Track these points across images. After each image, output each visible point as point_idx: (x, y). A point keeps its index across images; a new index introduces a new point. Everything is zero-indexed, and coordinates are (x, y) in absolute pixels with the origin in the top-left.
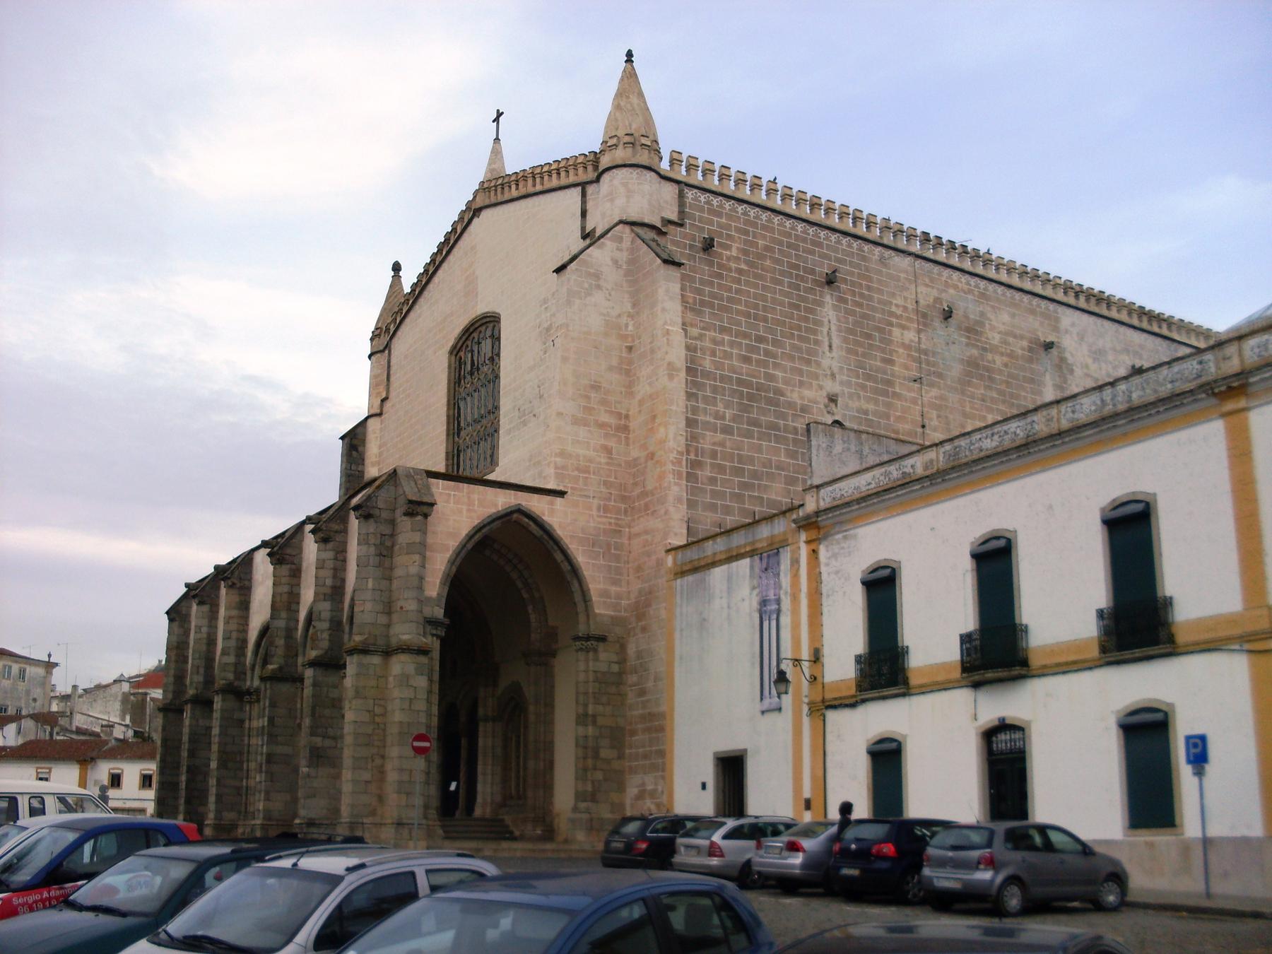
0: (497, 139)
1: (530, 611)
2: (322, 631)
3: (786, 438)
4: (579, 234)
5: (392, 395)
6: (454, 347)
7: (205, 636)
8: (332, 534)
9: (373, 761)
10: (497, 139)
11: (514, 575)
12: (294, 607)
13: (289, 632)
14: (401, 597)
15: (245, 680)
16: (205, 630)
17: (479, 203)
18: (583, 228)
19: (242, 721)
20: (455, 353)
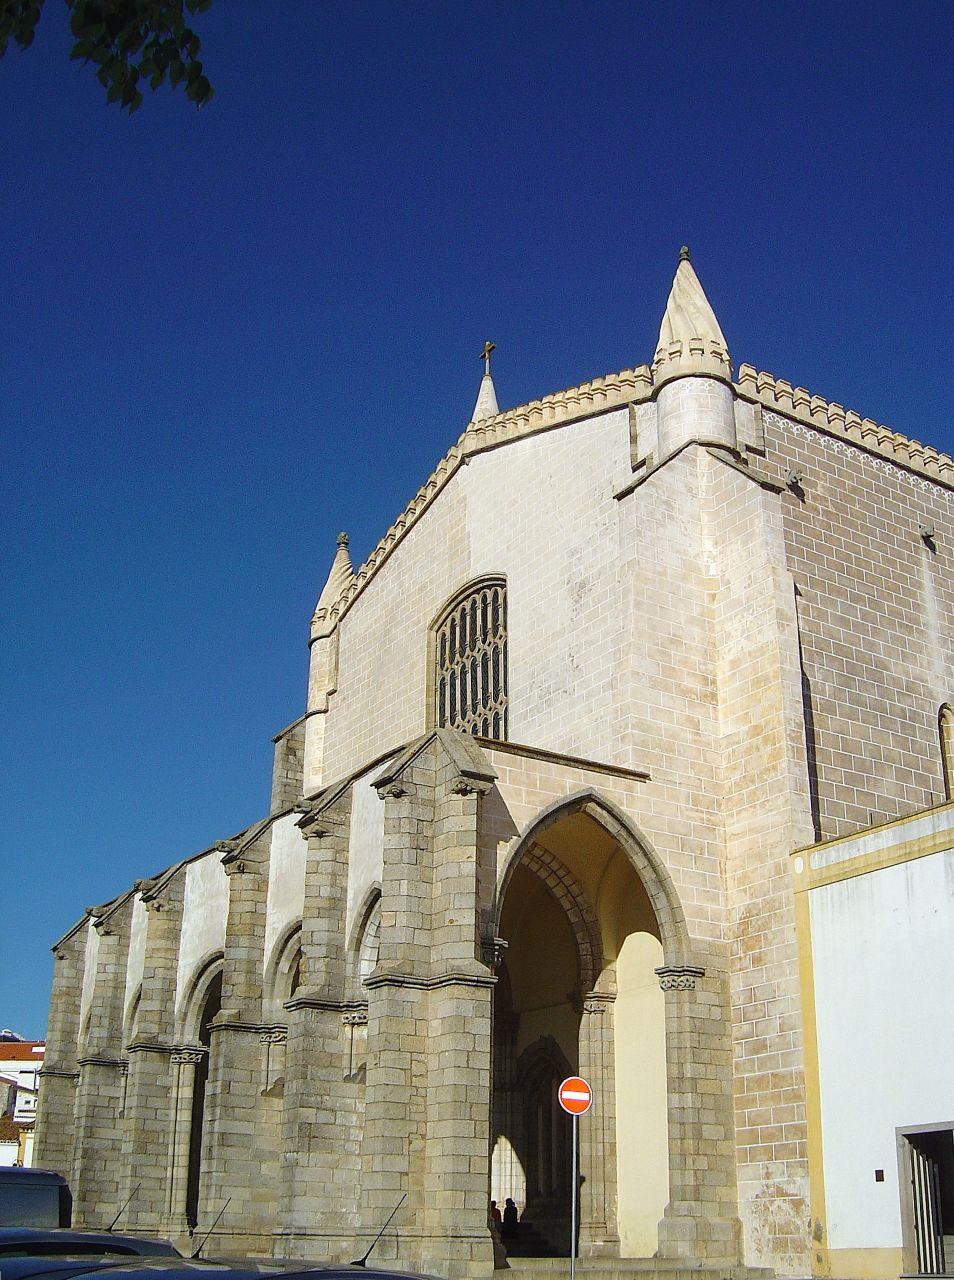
3: (894, 722)
7: (111, 976)
9: (410, 1143)
11: (558, 892)
12: (258, 931)
13: (252, 966)
15: (173, 1033)
16: (111, 969)
18: (633, 456)
19: (168, 1089)
20: (436, 627)
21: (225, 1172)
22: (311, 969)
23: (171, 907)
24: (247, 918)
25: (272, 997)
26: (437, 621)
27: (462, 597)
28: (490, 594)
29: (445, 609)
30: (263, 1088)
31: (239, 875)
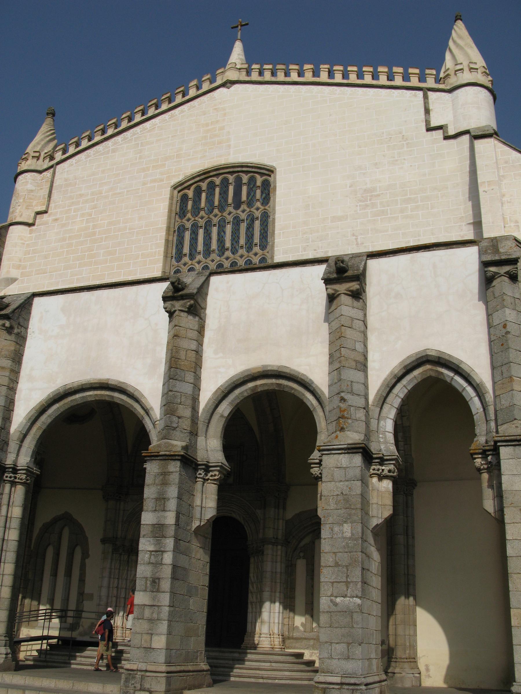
4: (423, 127)
6: (181, 184)
13: (195, 399)
18: (428, 122)
20: (180, 188)
22: (353, 417)
23: (19, 331)
27: (215, 173)
29: (193, 178)
31: (186, 314)
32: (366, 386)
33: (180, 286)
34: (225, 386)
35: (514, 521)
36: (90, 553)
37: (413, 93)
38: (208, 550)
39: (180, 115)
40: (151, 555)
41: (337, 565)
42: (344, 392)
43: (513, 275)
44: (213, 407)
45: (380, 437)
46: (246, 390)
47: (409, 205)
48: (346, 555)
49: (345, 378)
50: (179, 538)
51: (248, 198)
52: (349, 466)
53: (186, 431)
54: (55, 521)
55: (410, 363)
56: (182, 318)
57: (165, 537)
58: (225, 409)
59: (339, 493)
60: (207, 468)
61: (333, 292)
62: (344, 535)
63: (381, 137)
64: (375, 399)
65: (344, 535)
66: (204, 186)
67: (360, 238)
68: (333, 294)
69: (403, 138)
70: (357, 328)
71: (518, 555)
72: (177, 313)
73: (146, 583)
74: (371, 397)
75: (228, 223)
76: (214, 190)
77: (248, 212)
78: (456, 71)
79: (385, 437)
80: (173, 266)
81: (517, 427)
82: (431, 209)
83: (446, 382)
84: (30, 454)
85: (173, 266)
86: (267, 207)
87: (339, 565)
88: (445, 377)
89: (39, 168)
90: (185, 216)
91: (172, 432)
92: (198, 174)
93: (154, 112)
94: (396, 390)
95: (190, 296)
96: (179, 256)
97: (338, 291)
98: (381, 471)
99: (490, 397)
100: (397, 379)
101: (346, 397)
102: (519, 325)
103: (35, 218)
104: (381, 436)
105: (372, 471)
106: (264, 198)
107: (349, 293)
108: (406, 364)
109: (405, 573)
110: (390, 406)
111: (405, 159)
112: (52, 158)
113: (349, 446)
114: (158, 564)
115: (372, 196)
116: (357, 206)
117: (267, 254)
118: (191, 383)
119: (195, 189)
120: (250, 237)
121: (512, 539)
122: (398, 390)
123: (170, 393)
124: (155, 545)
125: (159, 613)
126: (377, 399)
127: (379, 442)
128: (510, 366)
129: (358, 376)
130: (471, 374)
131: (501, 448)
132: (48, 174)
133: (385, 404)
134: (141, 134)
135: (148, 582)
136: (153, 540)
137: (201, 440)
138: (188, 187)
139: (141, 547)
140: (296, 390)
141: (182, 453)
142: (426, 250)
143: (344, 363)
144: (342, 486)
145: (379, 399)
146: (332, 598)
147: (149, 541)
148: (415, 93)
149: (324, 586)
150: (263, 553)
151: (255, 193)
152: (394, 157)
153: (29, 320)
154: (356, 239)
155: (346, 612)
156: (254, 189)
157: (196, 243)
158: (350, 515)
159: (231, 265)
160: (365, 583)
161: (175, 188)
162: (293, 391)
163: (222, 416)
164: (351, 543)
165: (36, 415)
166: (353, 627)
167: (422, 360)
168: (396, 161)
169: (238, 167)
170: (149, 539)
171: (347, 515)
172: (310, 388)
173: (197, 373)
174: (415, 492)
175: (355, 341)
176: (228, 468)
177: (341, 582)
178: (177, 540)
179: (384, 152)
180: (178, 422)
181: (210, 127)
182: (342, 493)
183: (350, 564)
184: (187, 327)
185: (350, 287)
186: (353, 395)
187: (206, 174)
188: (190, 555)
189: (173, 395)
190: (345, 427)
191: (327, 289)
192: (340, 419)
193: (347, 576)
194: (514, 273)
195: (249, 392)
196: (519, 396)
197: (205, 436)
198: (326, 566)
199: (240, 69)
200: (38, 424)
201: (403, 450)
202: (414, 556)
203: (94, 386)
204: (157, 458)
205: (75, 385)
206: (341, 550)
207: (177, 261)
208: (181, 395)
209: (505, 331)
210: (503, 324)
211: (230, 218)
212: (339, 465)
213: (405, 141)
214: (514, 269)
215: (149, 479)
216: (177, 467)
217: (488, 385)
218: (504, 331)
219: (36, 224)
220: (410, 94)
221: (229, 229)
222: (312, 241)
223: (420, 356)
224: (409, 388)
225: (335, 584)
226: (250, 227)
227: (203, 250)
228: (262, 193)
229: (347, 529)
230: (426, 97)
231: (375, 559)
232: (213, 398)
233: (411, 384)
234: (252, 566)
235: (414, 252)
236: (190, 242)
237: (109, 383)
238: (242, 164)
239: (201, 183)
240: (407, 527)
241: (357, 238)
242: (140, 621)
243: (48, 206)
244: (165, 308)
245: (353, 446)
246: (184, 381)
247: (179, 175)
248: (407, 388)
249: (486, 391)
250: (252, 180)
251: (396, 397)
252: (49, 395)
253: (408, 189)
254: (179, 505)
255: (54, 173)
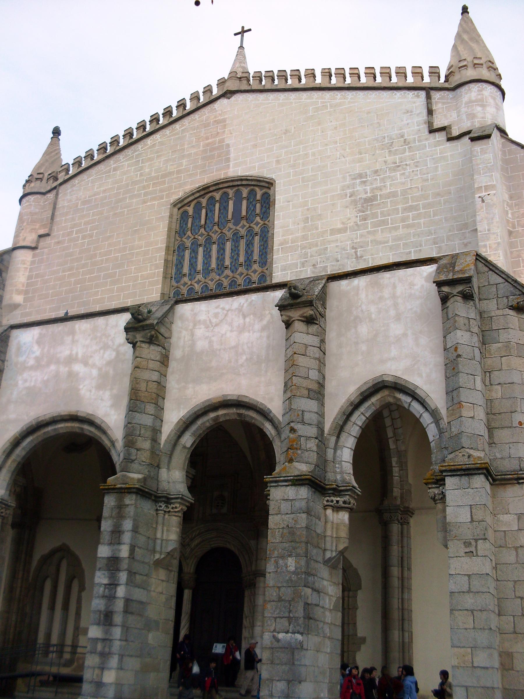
0: (241, 47)
1: (394, 464)
2: (308, 438)
5: (58, 232)
6: (181, 201)
8: (318, 315)
10: (241, 47)
13: (156, 431)
14: (519, 409)
17: (232, 86)
18: (430, 124)
20: (179, 205)
21: (126, 640)
22: (303, 447)
24: (153, 387)
25: (168, 469)
26: (183, 200)
28: (245, 192)
29: (193, 194)
30: (157, 556)
32: (321, 415)
33: (140, 317)
34: (187, 417)
35: (457, 555)
36: (86, 585)
37: (416, 94)
38: (173, 583)
39: (181, 129)
40: (105, 589)
41: (280, 600)
42: (294, 422)
43: (466, 294)
44: (175, 438)
45: (336, 467)
46: (208, 421)
47: (411, 214)
48: (289, 590)
49: (295, 408)
50: (134, 571)
51: (247, 212)
52: (295, 498)
53: (144, 463)
54: (53, 552)
55: (366, 390)
56: (144, 349)
57: (120, 571)
58: (188, 440)
59: (285, 526)
60: (168, 500)
61: (287, 318)
62: (288, 569)
63: (383, 142)
64: (331, 428)
65: (288, 569)
66: (204, 201)
67: (360, 250)
68: (288, 321)
69: (405, 142)
70: (311, 355)
71: (460, 590)
72: (138, 344)
73: (100, 616)
74: (327, 427)
75: (227, 239)
76: (214, 206)
77: (247, 228)
78: (459, 68)
79: (342, 467)
80: (173, 286)
81: (463, 455)
82: (433, 217)
83: (404, 408)
84: (5, 487)
85: (173, 286)
86: (266, 222)
87: (283, 600)
88: (403, 403)
89: (43, 191)
90: (185, 234)
91: (130, 464)
92: (198, 190)
93: (155, 127)
94: (354, 418)
95: (151, 327)
96: (179, 275)
97: (292, 318)
98: (335, 502)
99: (444, 423)
100: (353, 406)
101: (295, 427)
102: (472, 347)
103: (38, 242)
104: (337, 466)
105: (326, 503)
106: (264, 213)
107: (303, 319)
108: (362, 390)
109: (399, 607)
110: (347, 434)
111: (406, 165)
112: (56, 179)
113: (296, 478)
114: (111, 598)
115: (372, 205)
116: (357, 217)
117: (266, 271)
118: (151, 415)
119: (195, 205)
120: (249, 253)
121: (454, 573)
122: (356, 418)
123: (129, 425)
124: (110, 578)
125: (110, 647)
126: (333, 428)
127: (335, 472)
128: (459, 392)
129: (312, 405)
130: (426, 400)
131: (446, 478)
132: (52, 195)
133: (342, 432)
134: (142, 151)
135: (102, 616)
136: (108, 573)
137: (163, 473)
138: (188, 204)
139: (97, 580)
140: (256, 419)
141: (137, 486)
142: (386, 270)
143: (295, 392)
144: (287, 519)
145: (336, 428)
146: (274, 633)
147: (104, 574)
148: (418, 93)
149: (267, 622)
150: (255, 585)
151: (255, 207)
152: (396, 163)
153: (6, 352)
154: (356, 253)
155: (287, 648)
156: (254, 203)
157: (196, 262)
158: (294, 548)
159: (230, 285)
160: (311, 618)
161: (175, 206)
162: (253, 421)
163: (184, 447)
164: (294, 578)
165: (10, 448)
166: (293, 664)
167: (379, 386)
168: (399, 166)
169: (237, 180)
170: (104, 572)
171: (291, 548)
172: (268, 417)
173: (159, 404)
174: (412, 521)
175: (309, 369)
176: (192, 499)
177: (283, 617)
178: (131, 573)
179: (386, 157)
180: (137, 454)
181: (210, 140)
182: (288, 526)
183: (293, 599)
184: (149, 357)
185: (303, 313)
186: (304, 425)
187: (205, 190)
188: (149, 588)
189: (132, 427)
190: (293, 457)
191: (281, 315)
192: (289, 450)
193: (290, 612)
194: (467, 293)
195: (211, 422)
196: (468, 423)
197: (166, 467)
198: (270, 601)
199: (240, 78)
200: (13, 457)
201: (397, 476)
202: (410, 589)
203: (65, 418)
204: (113, 491)
205: (47, 417)
206: (285, 585)
207: (177, 281)
208: (140, 427)
209: (456, 354)
210: (454, 347)
211: (229, 234)
212: (286, 497)
213: (407, 145)
214: (467, 289)
215: (106, 512)
216: (132, 499)
217: (443, 412)
218: (455, 354)
219: (39, 247)
220: (412, 95)
221: (228, 246)
222: (311, 257)
223: (376, 382)
224: (367, 415)
225: (278, 619)
226: (249, 244)
227: (203, 269)
228: (262, 206)
229: (291, 563)
230: (428, 97)
231: (330, 593)
232: (174, 428)
233: (369, 411)
234: (246, 599)
235: (375, 272)
236: (190, 261)
237: (78, 415)
238: (241, 178)
239: (201, 199)
240: (402, 558)
241: (357, 251)
242: (93, 655)
243: (51, 229)
244: (127, 339)
245: (299, 478)
246: (144, 413)
247: (179, 191)
248: (364, 416)
249: (440, 417)
250: (252, 193)
251: (353, 425)
252: (23, 427)
253: (410, 196)
254: (133, 538)
255: (57, 194)
